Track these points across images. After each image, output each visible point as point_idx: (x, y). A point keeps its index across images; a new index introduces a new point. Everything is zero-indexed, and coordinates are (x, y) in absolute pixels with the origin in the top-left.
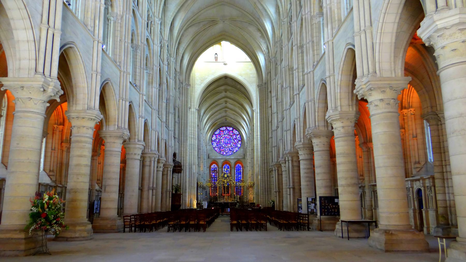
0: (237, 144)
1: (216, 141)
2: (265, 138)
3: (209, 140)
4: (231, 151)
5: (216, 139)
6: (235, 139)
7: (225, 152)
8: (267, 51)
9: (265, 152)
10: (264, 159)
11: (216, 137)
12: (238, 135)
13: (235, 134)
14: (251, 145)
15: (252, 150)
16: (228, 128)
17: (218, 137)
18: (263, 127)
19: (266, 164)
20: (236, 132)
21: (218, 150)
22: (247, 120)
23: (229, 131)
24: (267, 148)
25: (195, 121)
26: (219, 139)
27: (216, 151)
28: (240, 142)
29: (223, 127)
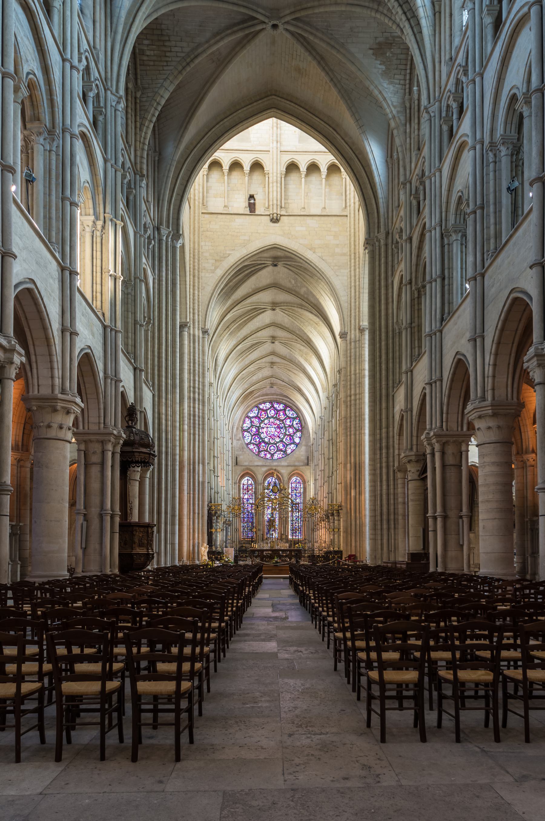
0: (292, 436)
1: (251, 430)
2: (384, 383)
3: (237, 429)
4: (281, 450)
5: (252, 426)
6: (291, 426)
7: (270, 453)
8: (402, 118)
9: (384, 421)
10: (381, 439)
11: (252, 422)
12: (296, 418)
13: (289, 418)
14: (326, 434)
15: (329, 441)
16: (276, 406)
17: (256, 421)
18: (378, 354)
19: (384, 451)
20: (291, 413)
21: (256, 450)
22: (319, 379)
23: (278, 411)
24: (387, 408)
25: (203, 360)
26: (258, 427)
27: (251, 450)
28: (299, 434)
29: (264, 403)
